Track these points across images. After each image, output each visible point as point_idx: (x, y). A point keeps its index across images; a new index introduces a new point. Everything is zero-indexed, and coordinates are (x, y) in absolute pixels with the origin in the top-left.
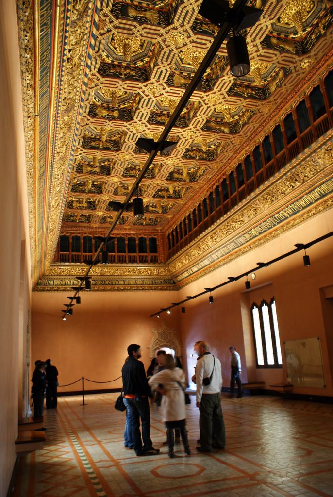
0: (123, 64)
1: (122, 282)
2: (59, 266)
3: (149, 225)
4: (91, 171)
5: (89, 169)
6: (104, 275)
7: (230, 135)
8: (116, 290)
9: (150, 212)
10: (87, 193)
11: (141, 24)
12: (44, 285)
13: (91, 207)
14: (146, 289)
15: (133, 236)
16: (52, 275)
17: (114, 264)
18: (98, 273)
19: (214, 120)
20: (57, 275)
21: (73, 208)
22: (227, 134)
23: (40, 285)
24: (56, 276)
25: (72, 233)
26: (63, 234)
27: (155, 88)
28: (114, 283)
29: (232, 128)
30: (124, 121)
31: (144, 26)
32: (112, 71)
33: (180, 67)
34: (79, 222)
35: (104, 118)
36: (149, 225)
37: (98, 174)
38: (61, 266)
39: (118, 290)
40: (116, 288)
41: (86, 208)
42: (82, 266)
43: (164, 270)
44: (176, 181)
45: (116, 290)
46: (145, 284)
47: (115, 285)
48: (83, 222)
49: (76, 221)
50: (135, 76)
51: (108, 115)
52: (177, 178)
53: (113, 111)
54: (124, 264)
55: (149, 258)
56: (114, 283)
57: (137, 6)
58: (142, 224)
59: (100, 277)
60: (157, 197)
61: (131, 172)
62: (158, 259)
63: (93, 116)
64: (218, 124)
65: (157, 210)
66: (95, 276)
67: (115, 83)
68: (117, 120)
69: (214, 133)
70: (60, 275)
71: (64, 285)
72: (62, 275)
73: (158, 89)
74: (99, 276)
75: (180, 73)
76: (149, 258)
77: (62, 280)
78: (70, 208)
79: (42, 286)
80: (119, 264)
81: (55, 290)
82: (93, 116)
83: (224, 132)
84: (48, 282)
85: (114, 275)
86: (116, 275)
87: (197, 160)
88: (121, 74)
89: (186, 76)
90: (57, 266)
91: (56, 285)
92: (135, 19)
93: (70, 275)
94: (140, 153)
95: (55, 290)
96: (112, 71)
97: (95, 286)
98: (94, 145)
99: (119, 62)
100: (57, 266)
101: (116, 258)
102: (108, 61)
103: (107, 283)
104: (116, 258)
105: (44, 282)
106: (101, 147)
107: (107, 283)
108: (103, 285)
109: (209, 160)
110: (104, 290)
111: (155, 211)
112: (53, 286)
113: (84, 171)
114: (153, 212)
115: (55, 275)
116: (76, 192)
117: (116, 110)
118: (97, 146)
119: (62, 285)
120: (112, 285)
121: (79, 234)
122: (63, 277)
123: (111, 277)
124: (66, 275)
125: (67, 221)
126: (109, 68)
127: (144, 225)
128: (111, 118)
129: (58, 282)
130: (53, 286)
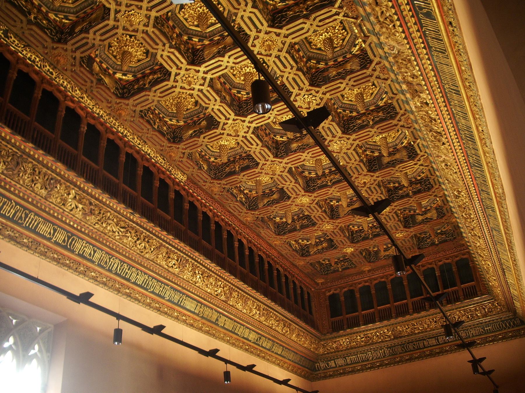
0: (147, 72)
1: (433, 342)
2: (333, 338)
3: (445, 241)
4: (269, 201)
5: (265, 201)
6: (401, 337)
7: (365, 71)
8: (428, 355)
9: (420, 224)
10: (299, 231)
11: (86, 31)
12: (324, 369)
13: (333, 246)
14: (479, 344)
15: (430, 266)
16: (328, 353)
17: (408, 317)
18: (389, 337)
19: (332, 63)
20: (335, 352)
21: (310, 255)
22: (358, 71)
23: (319, 370)
24: (334, 354)
25: (342, 288)
26: (331, 292)
27: (187, 76)
28: (421, 345)
29: (363, 59)
30: (214, 129)
31: (92, 31)
32: (136, 87)
33: (208, 35)
34: (343, 269)
35: (191, 137)
36: (445, 241)
37: (277, 203)
38: (336, 337)
39: (432, 355)
40: (428, 353)
41: (326, 248)
42: (364, 331)
43: (493, 305)
44: (387, 167)
45: (428, 355)
46: (473, 336)
47: (425, 347)
48: (348, 268)
49: (338, 271)
50: (160, 78)
51: (195, 132)
52: (388, 163)
53: (200, 123)
54: (423, 313)
55: (461, 293)
56: (421, 345)
57: (84, 17)
58: (433, 244)
59: (396, 341)
60: (398, 200)
61: (319, 182)
62: (478, 290)
63: (179, 141)
64: (340, 65)
65: (429, 215)
66: (386, 341)
67: (145, 98)
68: (206, 132)
69: (338, 81)
70: (338, 351)
71: (350, 364)
72: (342, 351)
73: (191, 76)
74: (393, 339)
75: (210, 41)
76: (461, 293)
77: (345, 358)
78: (306, 256)
79: (321, 372)
80: (416, 315)
81: (341, 374)
82: (179, 141)
83: (352, 72)
84: (328, 364)
85: (415, 334)
86: (419, 333)
87: (372, 127)
88: (145, 85)
89: (218, 40)
90: (330, 339)
91: (339, 366)
92: (81, 32)
93: (352, 348)
94: (287, 155)
95: (341, 374)
96: (136, 87)
97: (395, 356)
98: (229, 171)
99: (141, 74)
100: (330, 339)
101: (410, 306)
102: (130, 77)
103: (411, 347)
104: (410, 306)
105: (322, 365)
106: (237, 169)
107: (411, 347)
108: (406, 352)
109: (392, 118)
110: (411, 360)
111: (427, 219)
112: (337, 369)
113: (261, 205)
114: (423, 222)
115: (332, 353)
116: (285, 233)
117: (204, 120)
118: (233, 169)
119: (347, 364)
120: (420, 349)
121: (351, 286)
122: (343, 352)
123: (413, 337)
124: (347, 349)
125: (327, 274)
126: (134, 86)
127: (437, 245)
128: (198, 134)
129: (340, 362)
130: (337, 369)
